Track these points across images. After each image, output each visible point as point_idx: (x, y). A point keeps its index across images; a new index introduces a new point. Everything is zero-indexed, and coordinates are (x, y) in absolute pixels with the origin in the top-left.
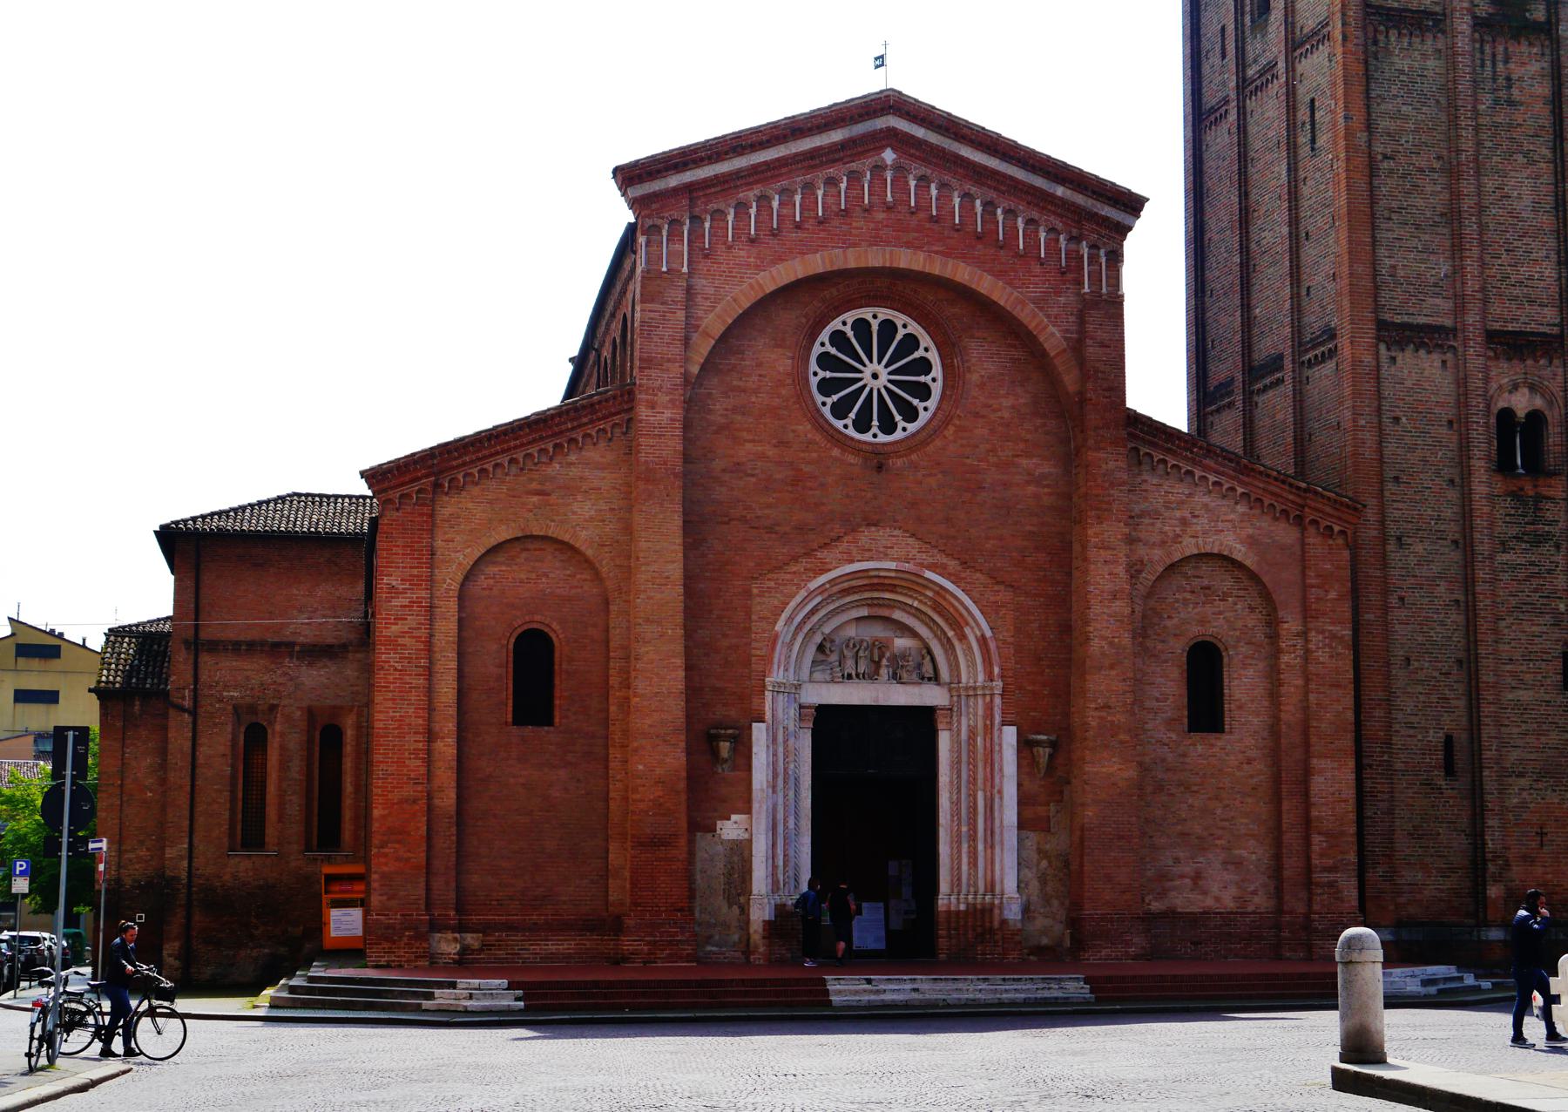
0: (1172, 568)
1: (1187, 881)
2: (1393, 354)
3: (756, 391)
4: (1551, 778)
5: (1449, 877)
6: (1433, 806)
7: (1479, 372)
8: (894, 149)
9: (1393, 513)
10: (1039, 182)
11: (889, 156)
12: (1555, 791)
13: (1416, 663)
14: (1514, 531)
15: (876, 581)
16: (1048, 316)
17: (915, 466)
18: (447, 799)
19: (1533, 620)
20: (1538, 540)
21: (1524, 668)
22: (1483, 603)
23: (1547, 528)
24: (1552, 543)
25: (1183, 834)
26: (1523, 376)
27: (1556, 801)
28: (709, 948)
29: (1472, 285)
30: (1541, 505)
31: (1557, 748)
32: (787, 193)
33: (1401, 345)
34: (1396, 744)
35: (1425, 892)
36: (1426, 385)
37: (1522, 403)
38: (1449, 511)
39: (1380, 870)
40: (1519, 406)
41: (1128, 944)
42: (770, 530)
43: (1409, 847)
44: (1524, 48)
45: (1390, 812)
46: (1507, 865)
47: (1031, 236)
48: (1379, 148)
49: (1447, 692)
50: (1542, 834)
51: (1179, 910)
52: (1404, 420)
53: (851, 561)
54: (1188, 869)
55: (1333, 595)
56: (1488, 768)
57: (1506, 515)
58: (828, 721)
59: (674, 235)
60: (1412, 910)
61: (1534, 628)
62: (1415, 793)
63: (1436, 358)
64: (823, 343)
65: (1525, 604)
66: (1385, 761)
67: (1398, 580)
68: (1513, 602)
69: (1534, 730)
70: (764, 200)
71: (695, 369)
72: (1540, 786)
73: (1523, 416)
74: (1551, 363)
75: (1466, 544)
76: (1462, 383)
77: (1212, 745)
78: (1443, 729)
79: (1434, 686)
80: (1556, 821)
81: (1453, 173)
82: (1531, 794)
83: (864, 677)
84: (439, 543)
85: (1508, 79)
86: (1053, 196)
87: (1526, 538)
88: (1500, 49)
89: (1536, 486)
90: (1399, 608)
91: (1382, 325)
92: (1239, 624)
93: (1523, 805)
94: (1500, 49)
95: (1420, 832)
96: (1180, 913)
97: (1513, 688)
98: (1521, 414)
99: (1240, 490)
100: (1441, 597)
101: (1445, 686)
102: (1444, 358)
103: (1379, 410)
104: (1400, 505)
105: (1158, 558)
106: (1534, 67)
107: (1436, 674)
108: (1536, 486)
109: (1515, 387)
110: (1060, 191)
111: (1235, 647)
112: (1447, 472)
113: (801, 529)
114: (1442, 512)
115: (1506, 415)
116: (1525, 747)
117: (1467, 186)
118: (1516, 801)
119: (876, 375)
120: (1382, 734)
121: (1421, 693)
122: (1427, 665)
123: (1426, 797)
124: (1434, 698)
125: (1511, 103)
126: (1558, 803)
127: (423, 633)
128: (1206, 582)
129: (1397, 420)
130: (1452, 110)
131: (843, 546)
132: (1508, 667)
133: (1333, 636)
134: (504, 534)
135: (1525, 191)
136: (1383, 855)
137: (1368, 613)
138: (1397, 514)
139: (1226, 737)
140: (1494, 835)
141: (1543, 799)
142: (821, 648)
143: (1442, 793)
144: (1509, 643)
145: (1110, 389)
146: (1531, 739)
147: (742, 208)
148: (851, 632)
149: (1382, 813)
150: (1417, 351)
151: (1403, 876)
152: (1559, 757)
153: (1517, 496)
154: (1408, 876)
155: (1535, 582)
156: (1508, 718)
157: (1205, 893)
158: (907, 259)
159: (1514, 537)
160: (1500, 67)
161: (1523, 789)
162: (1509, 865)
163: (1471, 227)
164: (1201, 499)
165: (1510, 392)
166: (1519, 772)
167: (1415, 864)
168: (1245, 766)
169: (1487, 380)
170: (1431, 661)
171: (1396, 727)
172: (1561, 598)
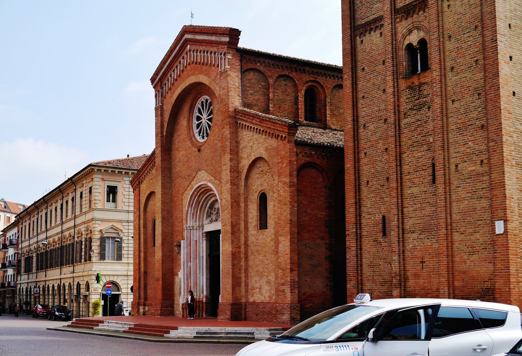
1: (258, 290)
2: (362, 39)
3: (181, 134)
4: (426, 232)
5: (384, 286)
6: (378, 251)
7: (389, 32)
9: (362, 114)
12: (428, 239)
13: (371, 183)
14: (409, 106)
15: (205, 189)
16: (216, 84)
17: (205, 148)
18: (142, 270)
19: (418, 150)
20: (420, 107)
21: (414, 176)
23: (424, 99)
24: (426, 107)
25: (258, 271)
26: (412, 24)
27: (430, 244)
28: (177, 312)
30: (421, 89)
31: (430, 216)
32: (174, 71)
33: (363, 34)
34: (364, 223)
35: (375, 293)
36: (374, 48)
37: (414, 39)
38: (383, 105)
39: (352, 283)
40: (414, 41)
41: (226, 313)
42: (184, 178)
43: (368, 272)
45: (359, 256)
46: (406, 279)
49: (383, 195)
50: (423, 262)
51: (256, 301)
52: (366, 68)
53: (197, 184)
54: (258, 285)
55: (285, 165)
56: (393, 230)
57: (407, 99)
61: (420, 154)
62: (370, 246)
63: (378, 32)
64: (196, 113)
65: (415, 142)
66: (354, 232)
67: (364, 145)
68: (410, 142)
69: (419, 208)
71: (165, 133)
72: (422, 236)
73: (416, 44)
74: (424, 12)
77: (264, 234)
78: (381, 213)
79: (378, 192)
80: (429, 255)
82: (418, 242)
83: (217, 221)
84: (141, 198)
86: (212, 41)
87: (415, 108)
89: (419, 79)
90: (365, 158)
92: (270, 183)
93: (414, 248)
95: (373, 264)
96: (257, 303)
97: (410, 187)
98: (415, 44)
99: (262, 129)
100: (380, 148)
101: (382, 192)
102: (381, 31)
104: (365, 109)
105: (245, 163)
107: (379, 186)
108: (419, 79)
109: (410, 32)
111: (269, 193)
113: (189, 176)
114: (380, 106)
116: (415, 217)
118: (411, 245)
120: (353, 219)
121: (373, 197)
122: (375, 183)
123: (375, 247)
124: (378, 199)
126: (431, 245)
127: (138, 224)
128: (262, 169)
129: (363, 69)
131: (195, 179)
132: (408, 177)
133: (285, 183)
134: (148, 192)
136: (353, 276)
137: (348, 164)
138: (364, 113)
139: (267, 230)
140: (395, 264)
141: (423, 243)
143: (381, 245)
144: (408, 164)
145: (226, 105)
146: (418, 213)
149: (353, 257)
150: (370, 33)
151: (366, 286)
152: (430, 220)
153: (410, 88)
155: (419, 129)
156: (408, 203)
157: (262, 295)
158: (193, 80)
159: (410, 109)
161: (414, 239)
162: (409, 279)
165: (409, 34)
166: (413, 231)
167: (371, 280)
168: (271, 242)
169: (394, 34)
170: (376, 181)
171: (363, 215)
172: (431, 135)
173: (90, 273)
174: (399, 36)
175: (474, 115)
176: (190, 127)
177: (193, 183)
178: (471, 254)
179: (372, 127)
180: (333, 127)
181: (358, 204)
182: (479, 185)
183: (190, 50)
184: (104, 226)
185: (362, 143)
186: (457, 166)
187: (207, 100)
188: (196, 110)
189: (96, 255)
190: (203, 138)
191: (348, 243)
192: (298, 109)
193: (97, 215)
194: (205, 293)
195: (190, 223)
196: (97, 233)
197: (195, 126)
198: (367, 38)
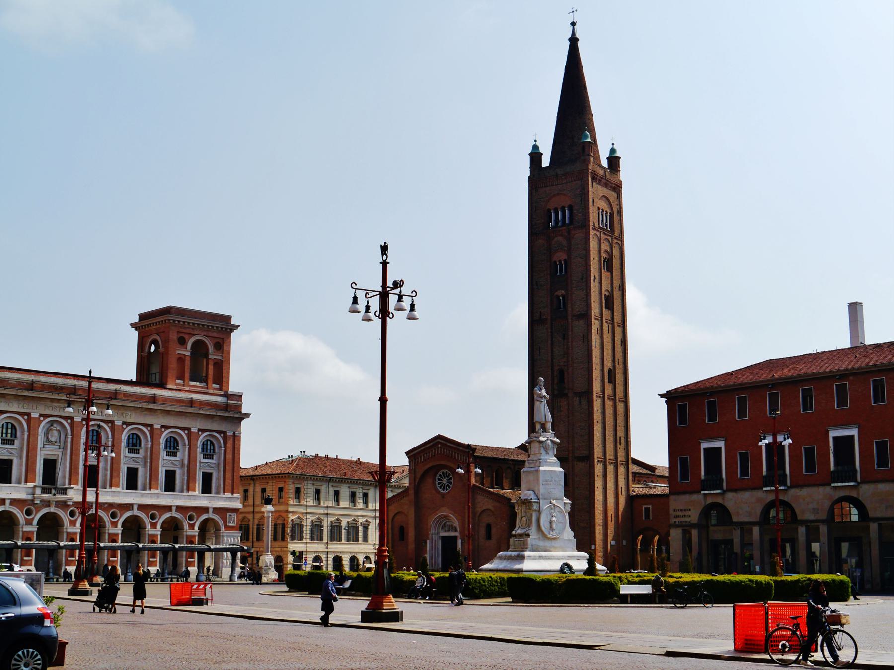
0: (483, 511)
8: (440, 444)
10: (458, 447)
11: (439, 445)
47: (458, 457)
58: (444, 539)
59: (412, 463)
64: (438, 477)
70: (423, 455)
71: (416, 484)
85: (560, 406)
88: (559, 400)
94: (559, 400)
105: (479, 510)
106: (565, 403)
110: (461, 448)
119: (445, 481)
134: (397, 512)
142: (442, 527)
147: (421, 457)
148: (448, 524)
158: (443, 463)
160: (559, 404)
164: (486, 499)
173: (285, 549)
176: (434, 483)
177: (437, 512)
180: (506, 488)
183: (440, 447)
184: (294, 517)
186: (577, 523)
187: (447, 472)
188: (438, 475)
189: (289, 537)
190: (443, 490)
192: (493, 481)
193: (291, 509)
194: (440, 566)
195: (432, 531)
196: (290, 521)
197: (437, 483)
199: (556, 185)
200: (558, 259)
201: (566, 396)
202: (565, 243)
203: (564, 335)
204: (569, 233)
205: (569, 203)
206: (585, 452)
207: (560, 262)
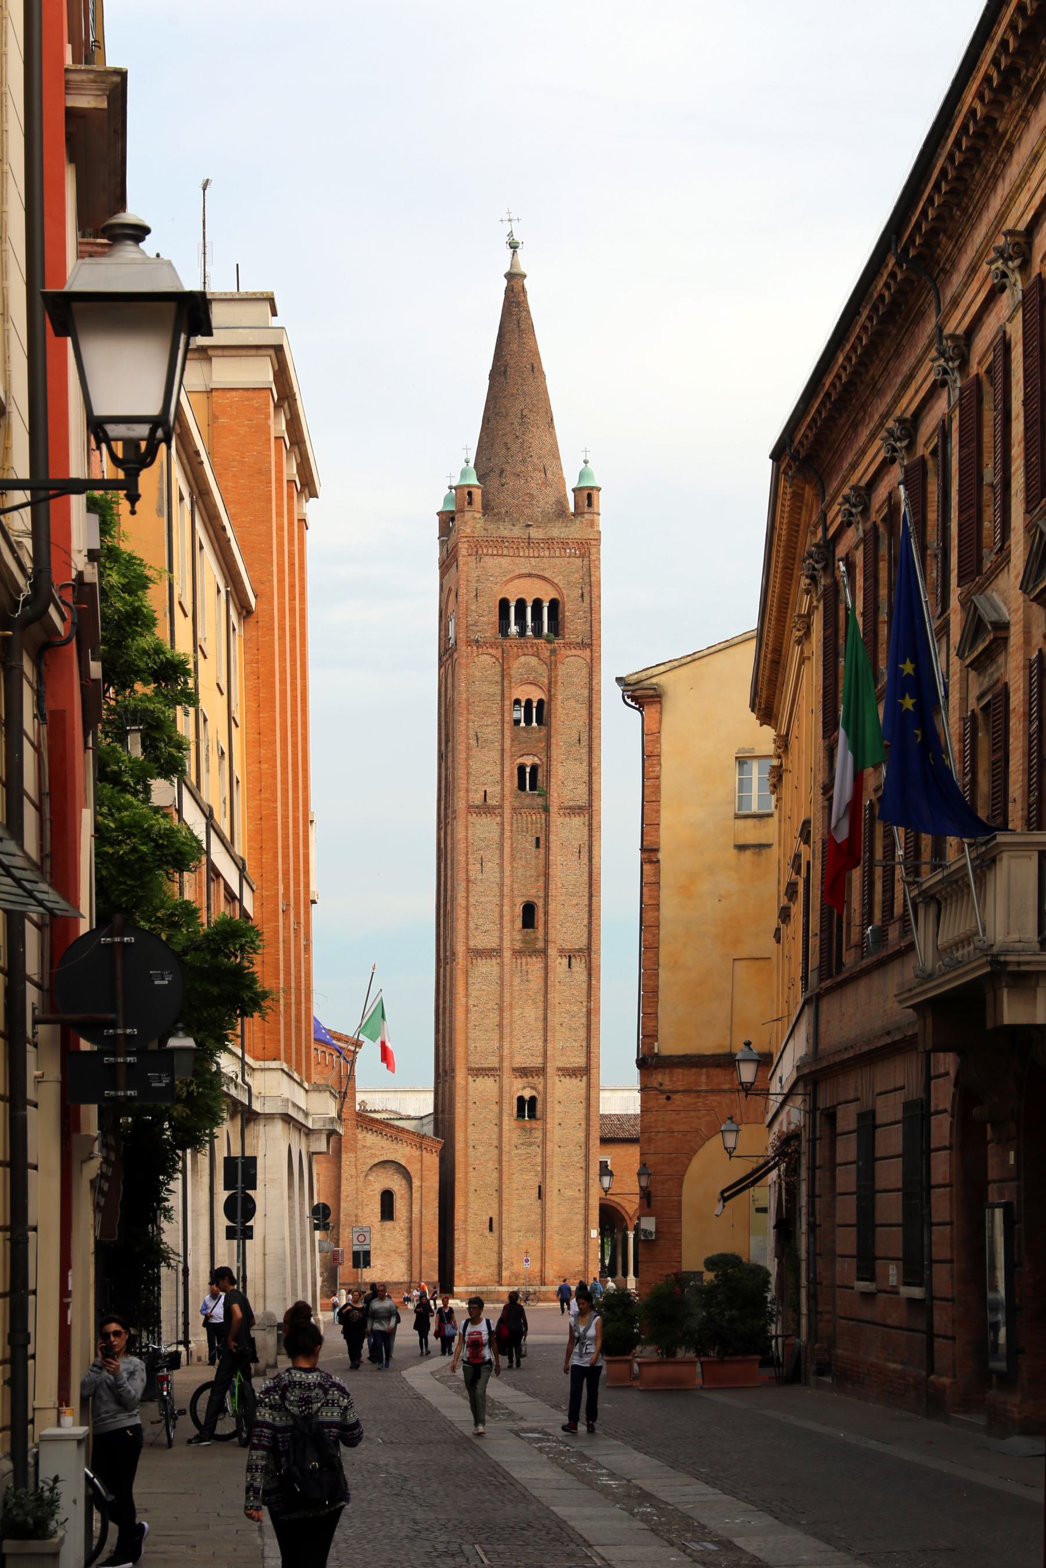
9: (471, 1137)
14: (520, 1141)
20: (531, 1144)
22: (505, 1169)
29: (506, 1052)
37: (527, 1094)
44: (534, 959)
45: (466, 1245)
48: (471, 1002)
60: (474, 1281)
75: (500, 1147)
76: (501, 1088)
81: (501, 1010)
91: (469, 1069)
98: (527, 1097)
103: (466, 1101)
109: (524, 1088)
112: (494, 1122)
115: (521, 1099)
117: (506, 1015)
125: (527, 981)
130: (502, 985)
135: (532, 1014)
153: (523, 1129)
154: (471, 1268)
160: (524, 967)
163: (507, 1030)
174: (514, 1089)
175: (576, 1159)
178: (566, 1249)
179: (481, 1149)
181: (466, 1207)
182: (576, 1205)
185: (471, 1160)
191: (456, 1236)
198: (480, 1080)
199: (524, 557)
200: (527, 697)
201: (544, 952)
202: (543, 669)
203: (538, 839)
204: (553, 652)
205: (553, 595)
206: (578, 1060)
207: (529, 702)
